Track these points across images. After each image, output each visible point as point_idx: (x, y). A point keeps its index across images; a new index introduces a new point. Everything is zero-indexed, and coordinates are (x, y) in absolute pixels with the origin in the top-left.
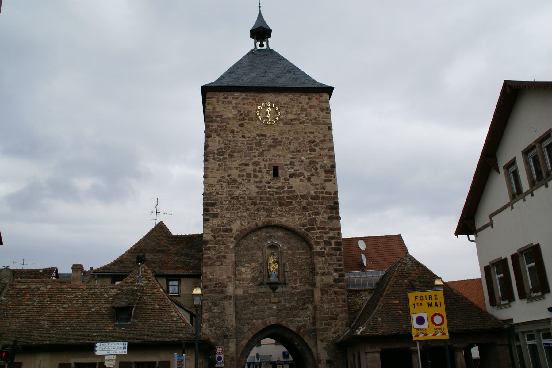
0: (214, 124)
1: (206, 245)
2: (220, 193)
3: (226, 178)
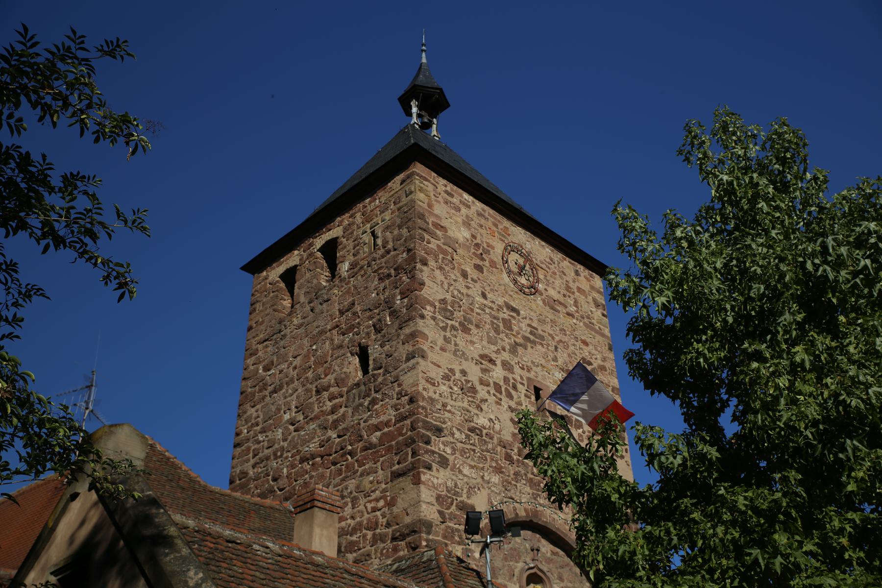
0: (432, 240)
1: (429, 533)
2: (449, 408)
3: (458, 375)
